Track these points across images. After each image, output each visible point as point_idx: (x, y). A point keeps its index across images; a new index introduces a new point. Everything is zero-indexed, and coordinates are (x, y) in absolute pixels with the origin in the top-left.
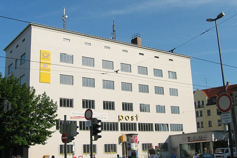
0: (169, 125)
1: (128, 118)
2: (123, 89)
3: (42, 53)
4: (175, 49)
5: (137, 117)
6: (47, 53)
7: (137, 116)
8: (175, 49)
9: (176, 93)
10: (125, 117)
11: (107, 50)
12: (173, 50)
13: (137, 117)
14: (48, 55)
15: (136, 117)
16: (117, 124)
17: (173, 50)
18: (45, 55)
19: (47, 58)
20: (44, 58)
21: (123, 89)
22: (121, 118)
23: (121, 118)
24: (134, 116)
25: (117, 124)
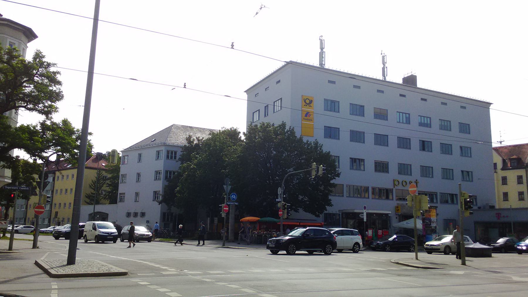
0: (438, 194)
1: (398, 183)
2: (376, 144)
3: (304, 99)
4: (504, 141)
5: (417, 183)
6: (309, 100)
7: (417, 182)
8: (504, 141)
9: (450, 152)
10: (406, 184)
11: (357, 90)
12: (502, 142)
13: (417, 183)
14: (311, 102)
15: (416, 183)
16: (392, 190)
17: (502, 142)
18: (308, 101)
19: (310, 105)
20: (307, 106)
21: (376, 144)
22: (396, 183)
23: (396, 183)
24: (414, 180)
25: (392, 190)
